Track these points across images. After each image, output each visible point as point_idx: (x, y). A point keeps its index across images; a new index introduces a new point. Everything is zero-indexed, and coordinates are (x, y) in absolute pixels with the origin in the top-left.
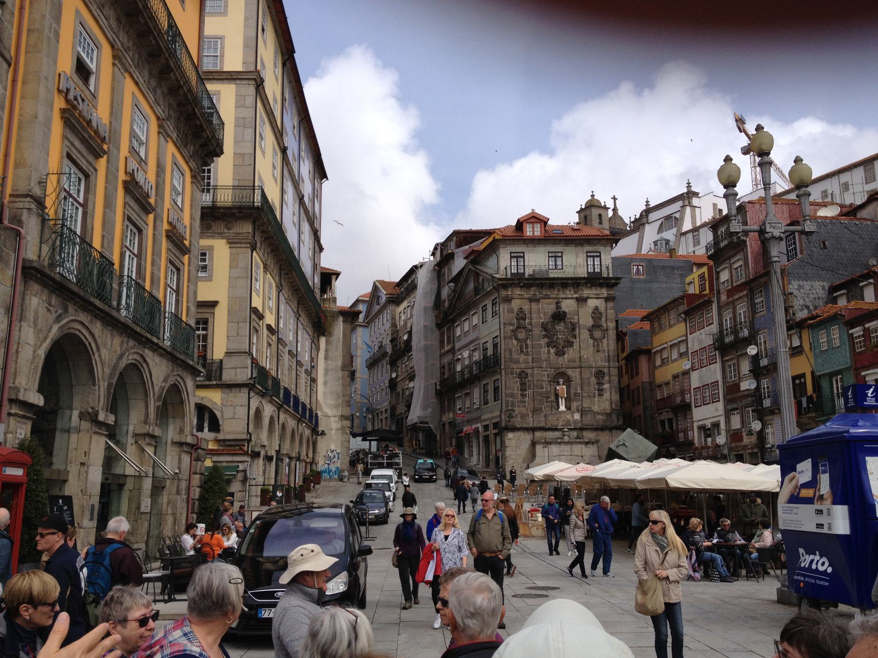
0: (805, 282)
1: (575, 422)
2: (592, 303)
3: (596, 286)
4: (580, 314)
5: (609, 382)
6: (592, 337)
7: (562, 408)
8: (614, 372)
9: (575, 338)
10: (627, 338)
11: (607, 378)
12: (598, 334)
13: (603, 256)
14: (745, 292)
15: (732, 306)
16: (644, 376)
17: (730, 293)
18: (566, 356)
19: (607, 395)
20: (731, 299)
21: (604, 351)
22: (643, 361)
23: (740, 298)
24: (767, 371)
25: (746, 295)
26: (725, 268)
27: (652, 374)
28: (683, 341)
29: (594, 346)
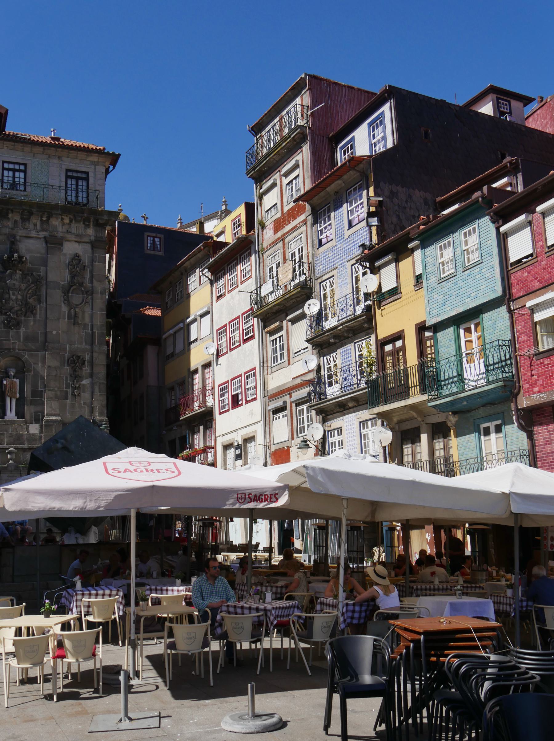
0: (399, 188)
1: (32, 438)
2: (71, 248)
3: (77, 221)
4: (49, 264)
5: (91, 375)
6: (67, 301)
7: (11, 415)
8: (101, 360)
9: (40, 301)
10: (131, 326)
11: (86, 369)
12: (76, 299)
13: (91, 180)
14: (302, 218)
15: (281, 244)
16: (152, 378)
17: (278, 225)
18: (22, 330)
19: (86, 396)
20: (279, 234)
21: (85, 327)
22: (151, 352)
23: (295, 228)
24: (335, 336)
25: (305, 222)
26: (274, 185)
27: (161, 373)
28: (207, 313)
29: (69, 317)
